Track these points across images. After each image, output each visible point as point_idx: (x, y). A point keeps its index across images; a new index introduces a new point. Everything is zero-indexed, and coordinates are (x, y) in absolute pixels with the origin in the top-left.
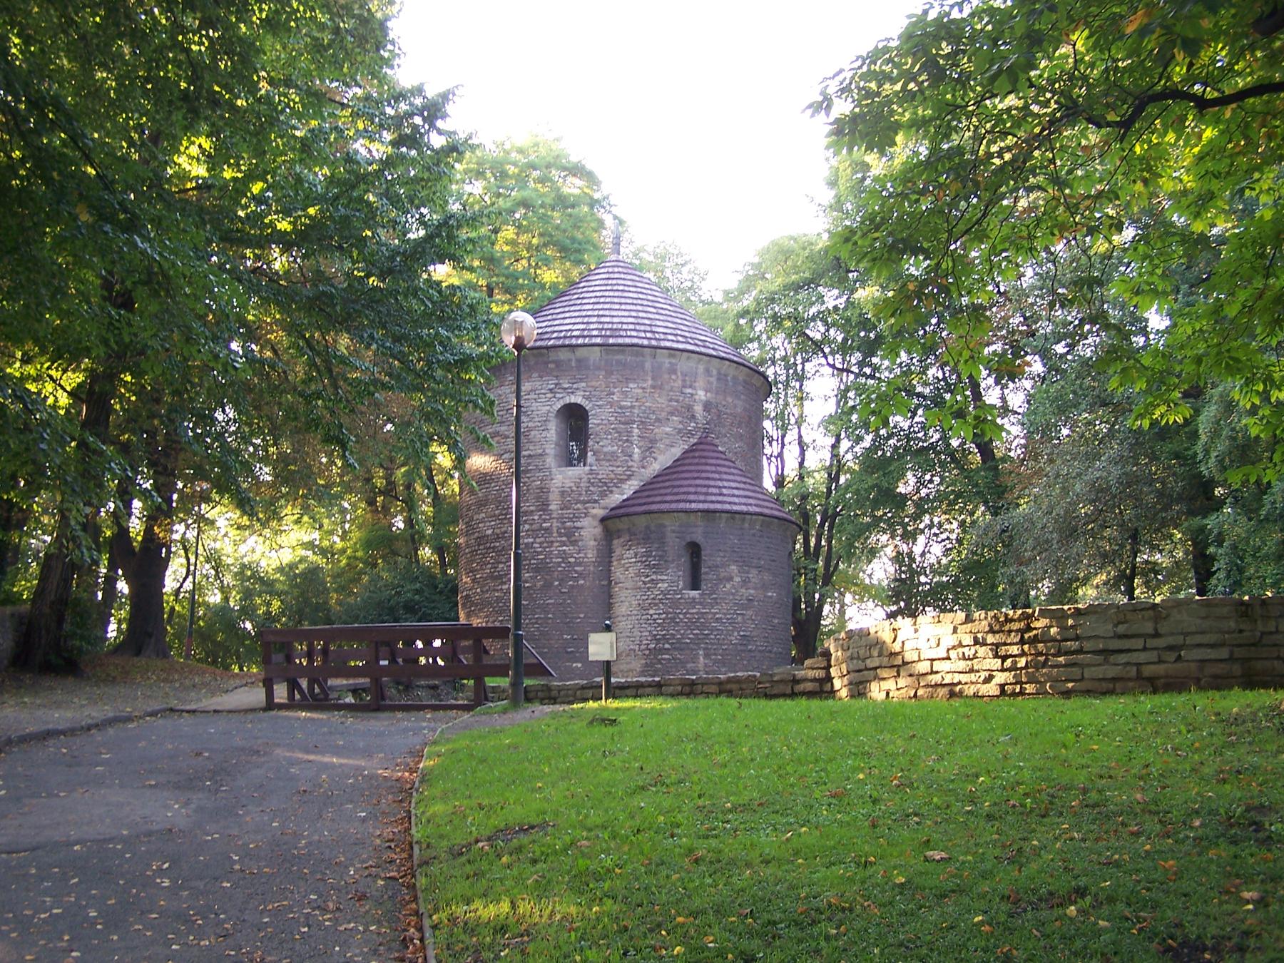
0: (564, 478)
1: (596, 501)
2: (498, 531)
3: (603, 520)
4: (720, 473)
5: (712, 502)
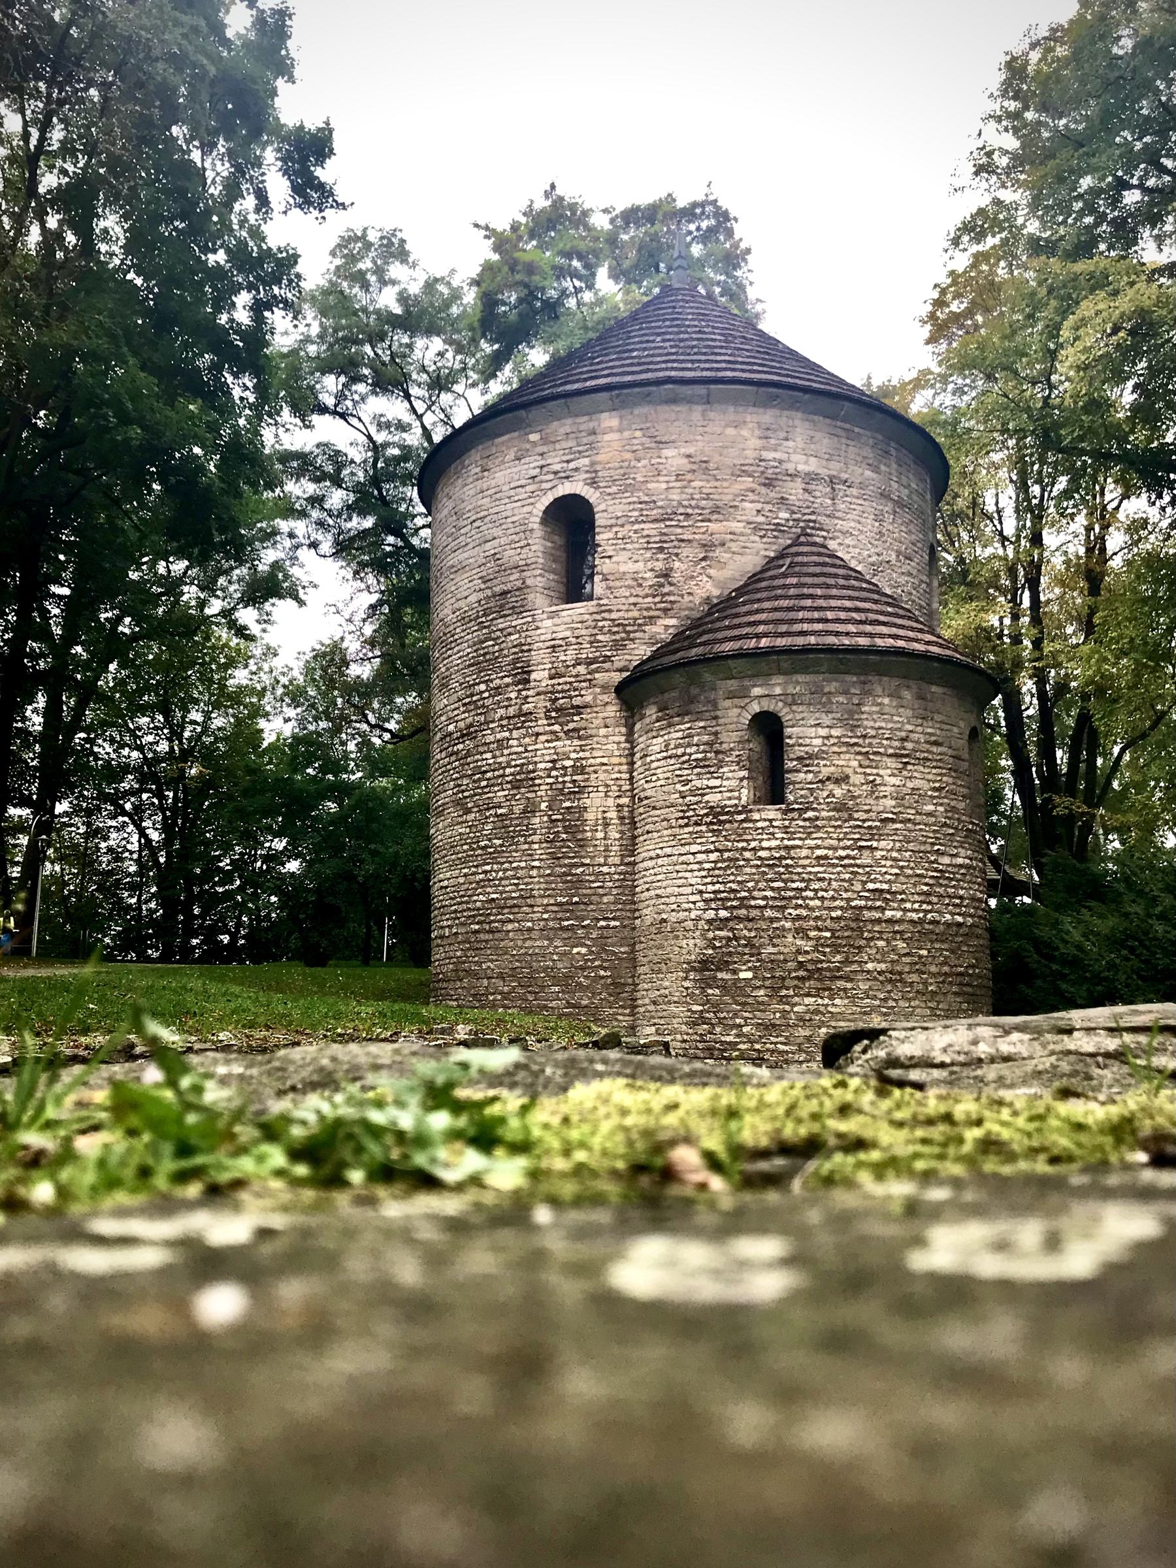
0: (554, 624)
1: (607, 659)
2: (462, 724)
3: (620, 689)
4: (828, 586)
5: (803, 633)
